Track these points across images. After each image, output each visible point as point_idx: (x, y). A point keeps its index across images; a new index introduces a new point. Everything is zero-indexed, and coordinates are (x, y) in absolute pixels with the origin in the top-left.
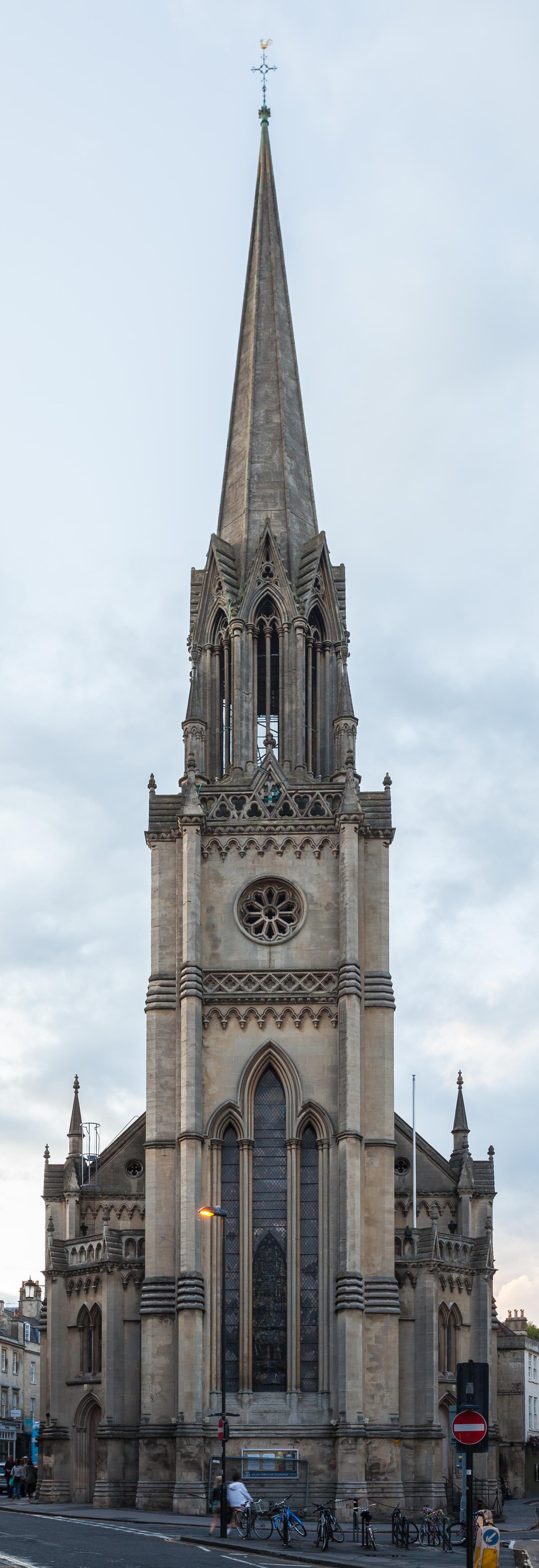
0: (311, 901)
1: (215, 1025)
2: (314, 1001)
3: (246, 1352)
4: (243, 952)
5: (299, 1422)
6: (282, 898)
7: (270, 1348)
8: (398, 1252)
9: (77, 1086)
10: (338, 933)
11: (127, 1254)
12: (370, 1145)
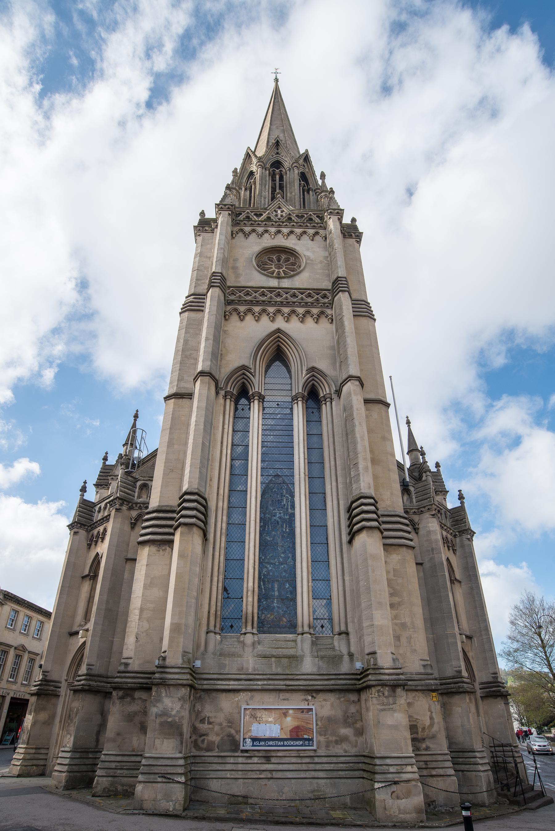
0: (308, 258)
1: (234, 318)
3: (251, 584)
5: (315, 670)
6: (287, 260)
9: (136, 416)
11: (139, 497)
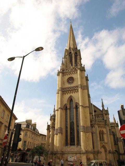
2: (76, 90)
4: (67, 85)
7: (71, 138)
8: (91, 123)
12: (85, 107)
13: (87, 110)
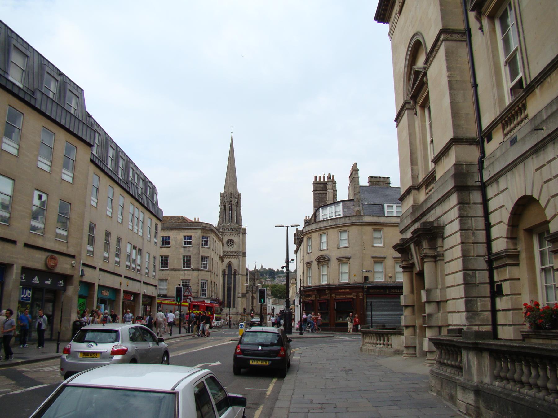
10: (239, 247)
13: (245, 277)
